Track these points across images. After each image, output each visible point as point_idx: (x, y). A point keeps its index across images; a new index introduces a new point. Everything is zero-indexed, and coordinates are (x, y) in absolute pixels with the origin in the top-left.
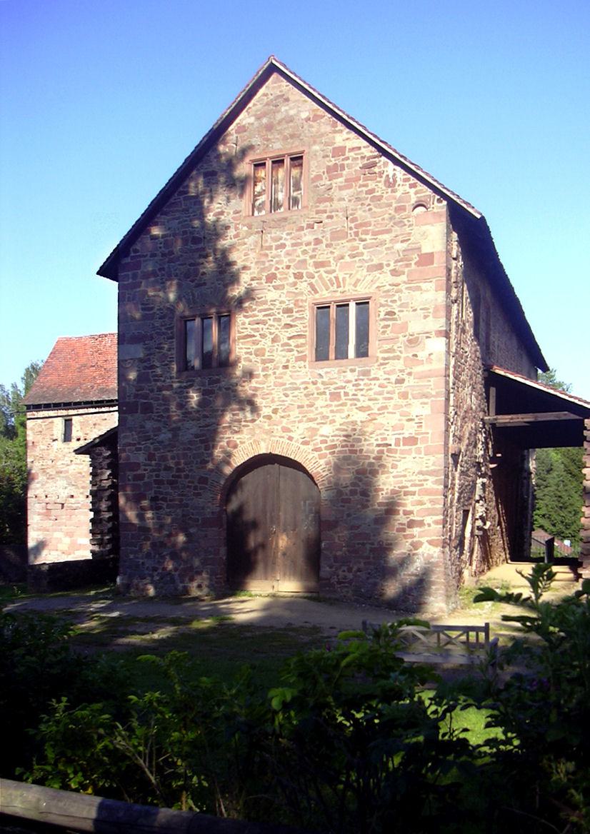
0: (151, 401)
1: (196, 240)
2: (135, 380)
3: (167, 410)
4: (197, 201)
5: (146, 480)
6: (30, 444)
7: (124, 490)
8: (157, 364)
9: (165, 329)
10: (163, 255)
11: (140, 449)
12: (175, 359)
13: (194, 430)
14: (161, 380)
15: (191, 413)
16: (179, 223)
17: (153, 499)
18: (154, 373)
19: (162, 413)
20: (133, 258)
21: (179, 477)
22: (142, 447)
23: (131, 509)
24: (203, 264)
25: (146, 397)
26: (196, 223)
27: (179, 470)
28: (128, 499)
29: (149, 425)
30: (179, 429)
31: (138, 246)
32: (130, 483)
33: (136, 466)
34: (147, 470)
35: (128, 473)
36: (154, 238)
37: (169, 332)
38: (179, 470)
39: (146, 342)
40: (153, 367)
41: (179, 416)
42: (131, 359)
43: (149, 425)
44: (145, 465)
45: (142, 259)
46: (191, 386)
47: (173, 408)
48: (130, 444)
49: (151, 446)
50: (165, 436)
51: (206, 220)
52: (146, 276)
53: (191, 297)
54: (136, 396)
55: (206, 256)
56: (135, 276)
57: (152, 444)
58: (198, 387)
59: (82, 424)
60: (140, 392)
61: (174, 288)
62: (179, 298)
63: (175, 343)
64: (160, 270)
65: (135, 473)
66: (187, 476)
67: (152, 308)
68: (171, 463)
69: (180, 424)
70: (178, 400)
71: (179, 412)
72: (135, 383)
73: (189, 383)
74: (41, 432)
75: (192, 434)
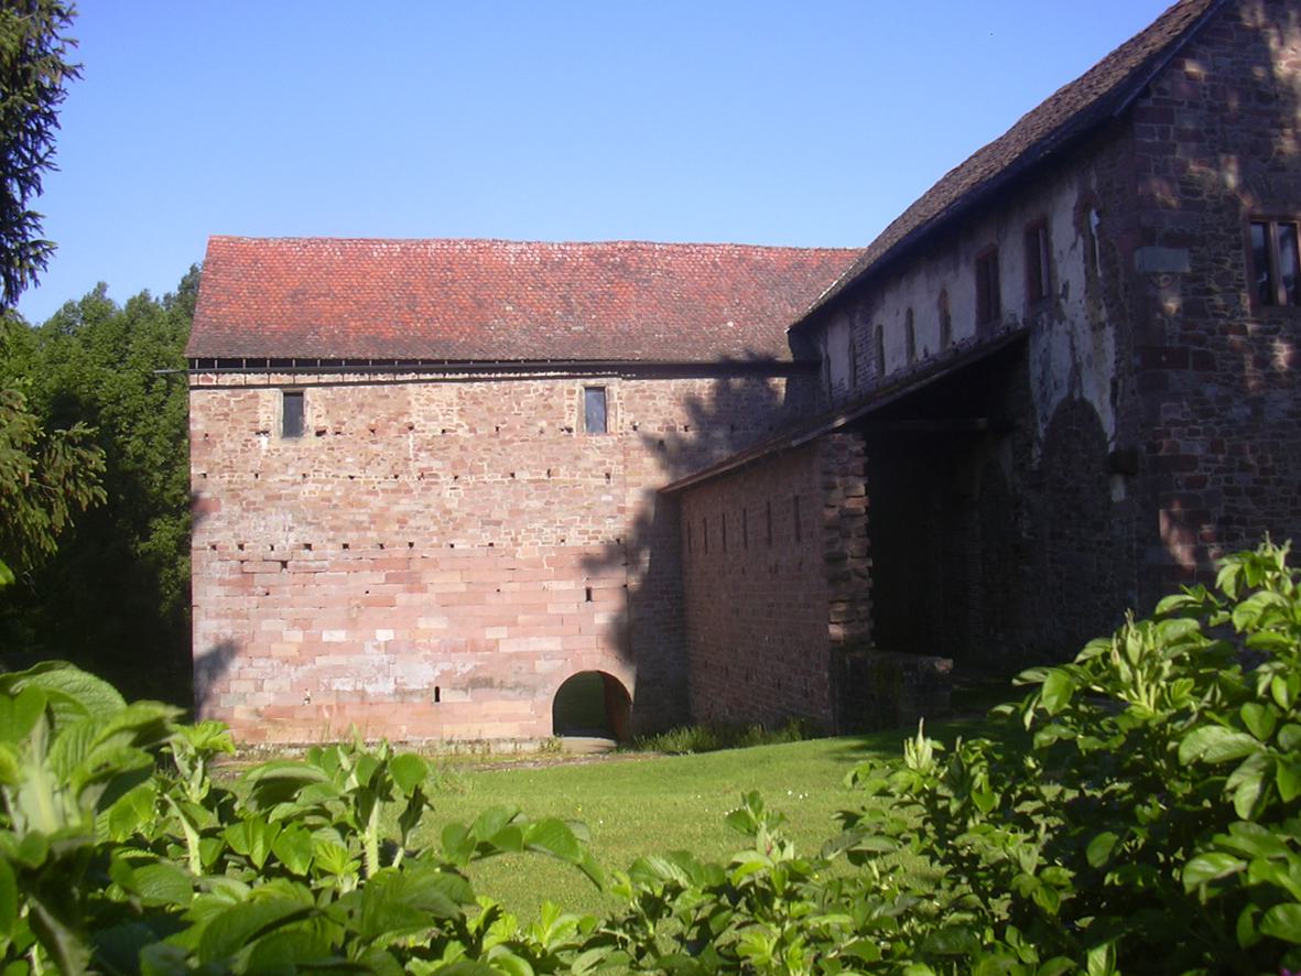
0: (1210, 349)
1: (1264, 98)
2: (1178, 310)
3: (1241, 367)
4: (1257, 37)
5: (1208, 486)
6: (197, 439)
7: (1168, 506)
8: (1214, 287)
9: (1225, 231)
10: (1211, 109)
11: (1197, 433)
12: (1246, 283)
13: (1286, 405)
14: (1225, 316)
15: (1278, 375)
16: (1233, 63)
17: (1224, 522)
18: (1211, 303)
19: (1230, 372)
20: (1156, 101)
21: (1267, 482)
22: (1201, 428)
23: (1182, 541)
24: (1277, 136)
25: (1201, 342)
26: (1260, 72)
27: (1264, 471)
28: (1173, 520)
29: (1210, 391)
30: (1262, 400)
31: (1166, 85)
32: (1184, 491)
33: (1191, 462)
34: (1210, 470)
35: (1176, 475)
36: (1190, 77)
37: (1233, 237)
38: (1264, 471)
39: (1195, 248)
40: (1209, 292)
41: (1260, 379)
42: (1168, 273)
43: (1210, 391)
44: (1207, 461)
45: (1175, 108)
46: (1276, 331)
47: (1249, 366)
48: (1175, 423)
49: (1217, 428)
50: (1239, 411)
51: (1276, 70)
52: (1184, 137)
53: (1265, 186)
54: (1183, 338)
55: (1282, 126)
56: (1164, 134)
57: (1218, 424)
58: (1287, 334)
59: (331, 406)
60: (1190, 332)
61: (1233, 167)
62: (1244, 186)
63: (1243, 257)
64: (1207, 131)
65: (1188, 474)
66: (1279, 482)
67: (1199, 193)
68: (1251, 460)
69: (1262, 393)
70: (1256, 352)
71: (1260, 373)
72: (1180, 315)
73: (1275, 326)
74: (226, 415)
75: (1283, 411)
